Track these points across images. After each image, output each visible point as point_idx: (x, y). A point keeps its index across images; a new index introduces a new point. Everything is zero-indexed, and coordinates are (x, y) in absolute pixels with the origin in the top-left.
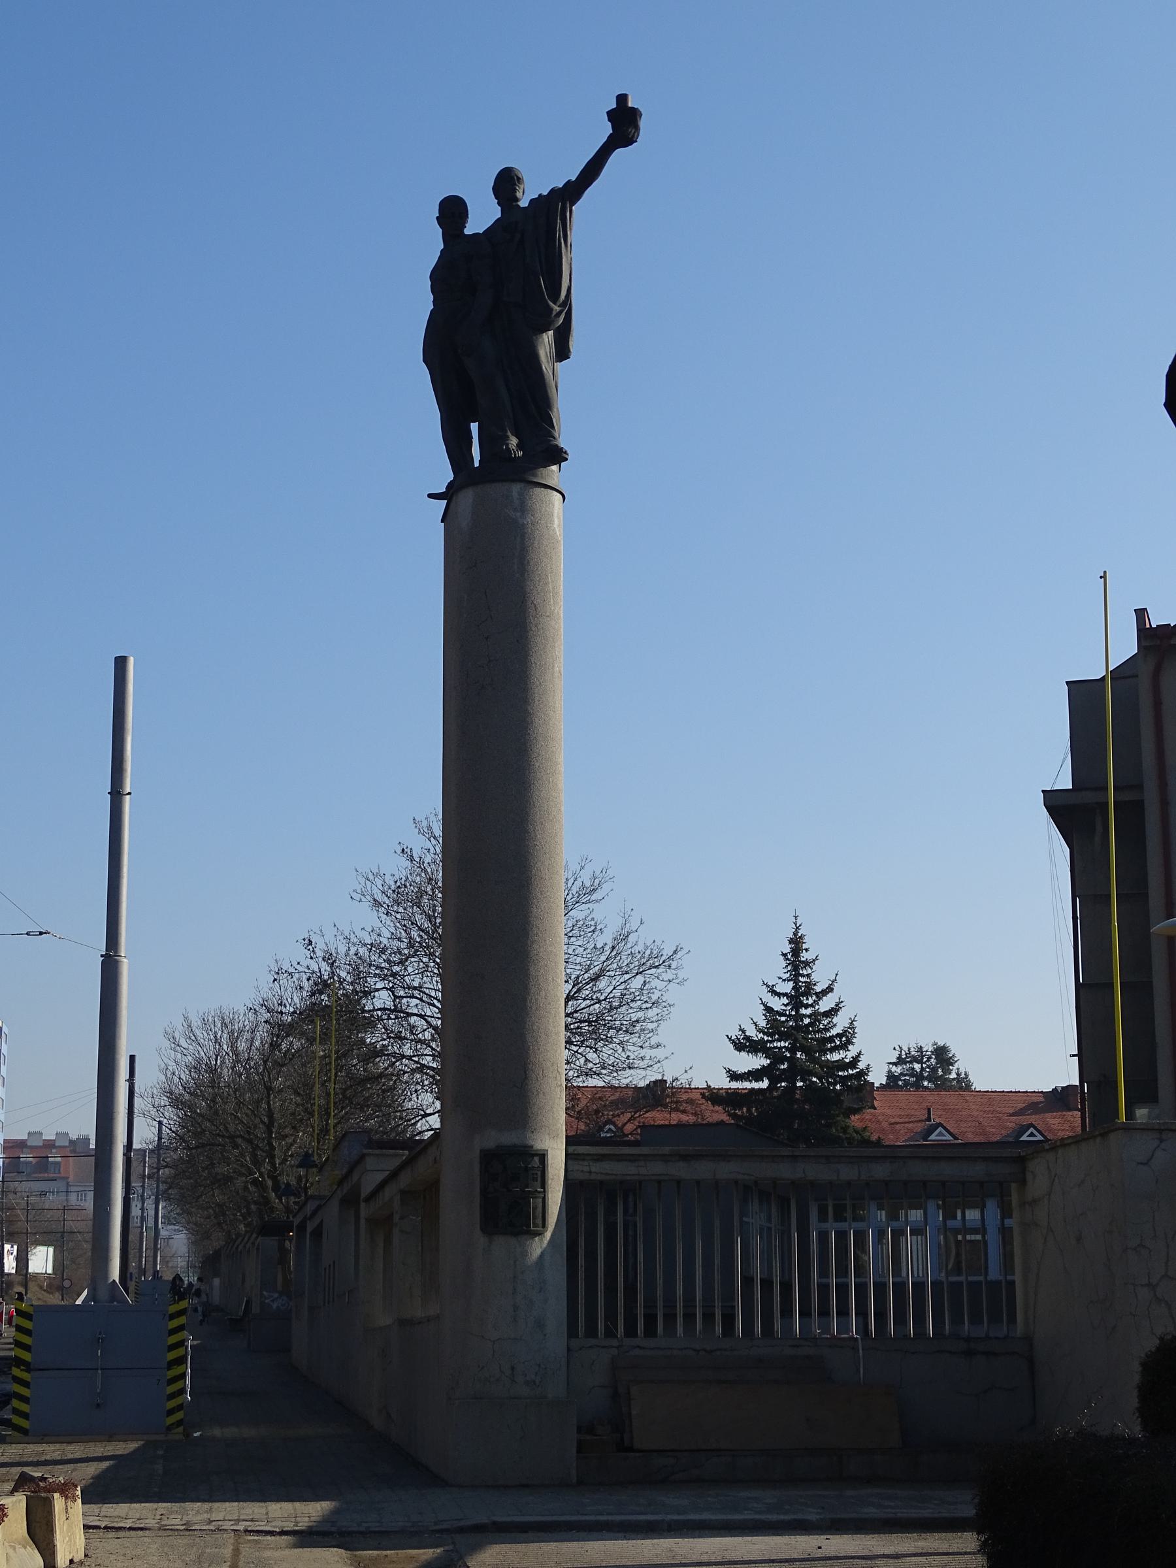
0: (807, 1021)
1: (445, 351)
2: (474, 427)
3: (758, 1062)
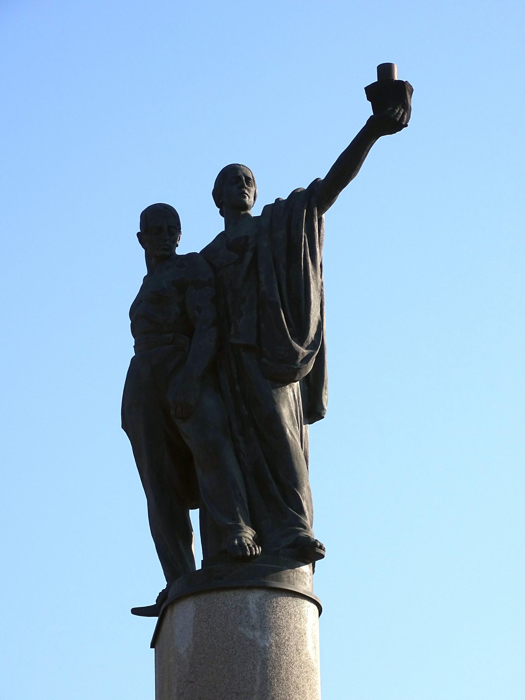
1: (152, 413)
2: (194, 515)
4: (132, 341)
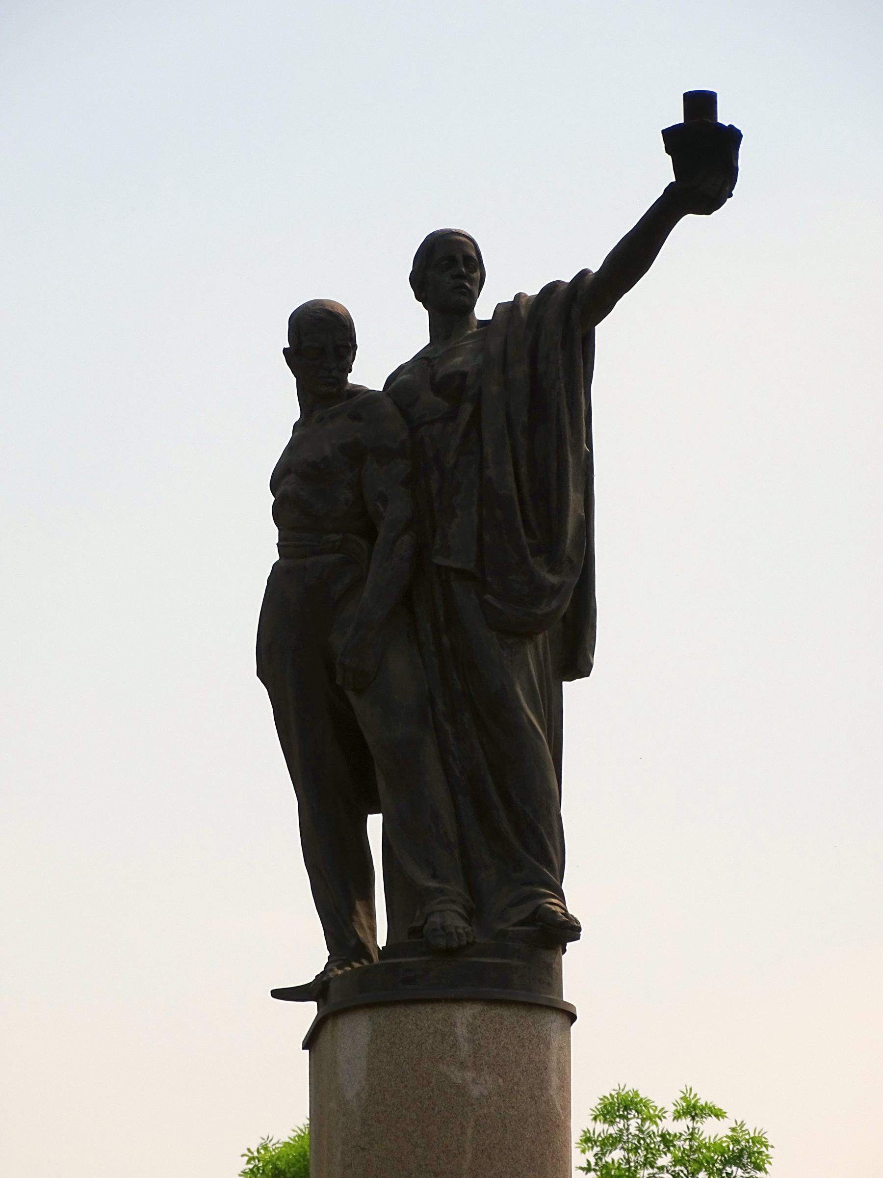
4: (273, 533)
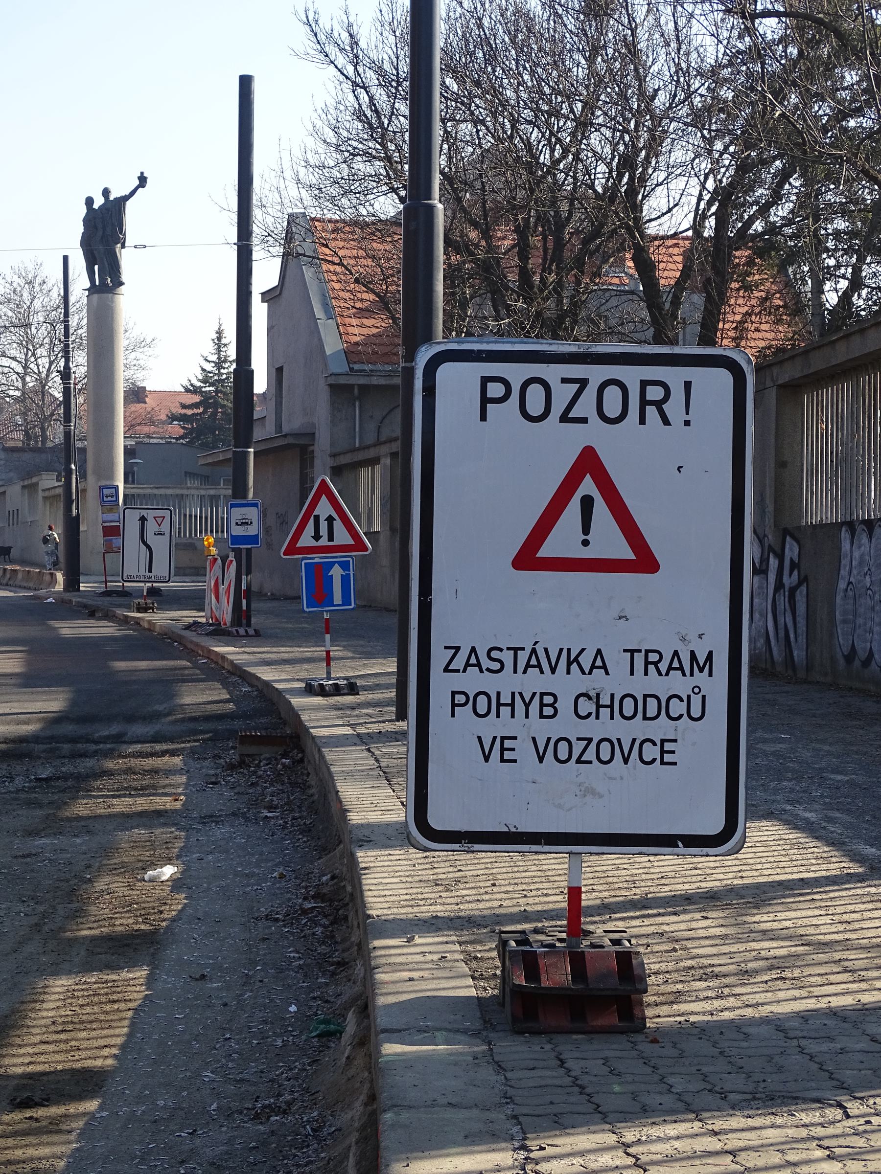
0: (224, 376)
3: (197, 399)
